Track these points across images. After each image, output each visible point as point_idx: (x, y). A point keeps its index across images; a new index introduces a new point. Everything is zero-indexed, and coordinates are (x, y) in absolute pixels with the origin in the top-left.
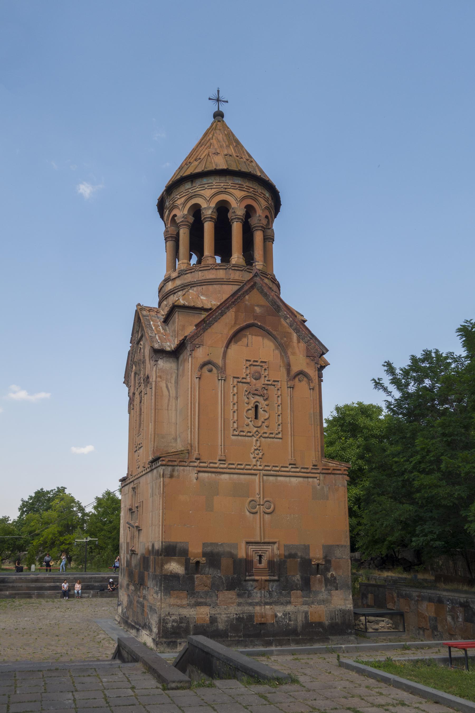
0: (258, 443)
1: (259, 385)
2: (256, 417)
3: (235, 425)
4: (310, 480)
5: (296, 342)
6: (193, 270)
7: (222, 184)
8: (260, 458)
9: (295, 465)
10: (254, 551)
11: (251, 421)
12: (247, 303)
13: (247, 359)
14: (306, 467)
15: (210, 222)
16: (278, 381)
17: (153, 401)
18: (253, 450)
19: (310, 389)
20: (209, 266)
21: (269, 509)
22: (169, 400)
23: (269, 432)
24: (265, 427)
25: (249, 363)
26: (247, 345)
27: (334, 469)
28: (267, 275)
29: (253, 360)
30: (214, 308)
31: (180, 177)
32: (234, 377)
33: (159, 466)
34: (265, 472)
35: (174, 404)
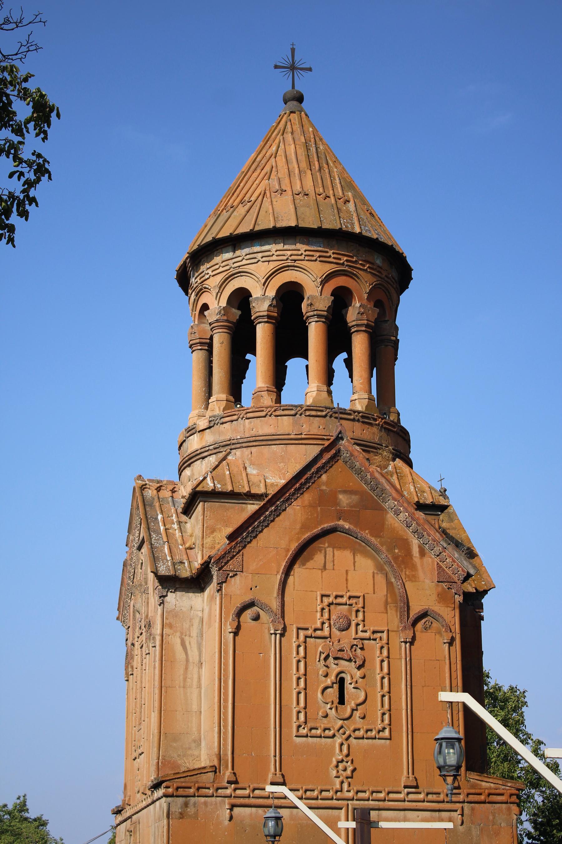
0: (345, 748)
1: (346, 641)
2: (342, 701)
3: (302, 716)
5: (418, 555)
6: (235, 417)
7: (289, 253)
8: (347, 778)
9: (417, 787)
12: (324, 488)
13: (324, 593)
14: (435, 790)
15: (267, 324)
16: (383, 632)
17: (157, 671)
18: (334, 762)
19: (445, 643)
20: (263, 411)
22: (186, 669)
24: (357, 718)
25: (326, 601)
26: (325, 567)
27: (489, 794)
28: (375, 420)
29: (334, 594)
30: (272, 492)
31: (209, 239)
33: (162, 797)
34: (358, 802)
35: (196, 676)
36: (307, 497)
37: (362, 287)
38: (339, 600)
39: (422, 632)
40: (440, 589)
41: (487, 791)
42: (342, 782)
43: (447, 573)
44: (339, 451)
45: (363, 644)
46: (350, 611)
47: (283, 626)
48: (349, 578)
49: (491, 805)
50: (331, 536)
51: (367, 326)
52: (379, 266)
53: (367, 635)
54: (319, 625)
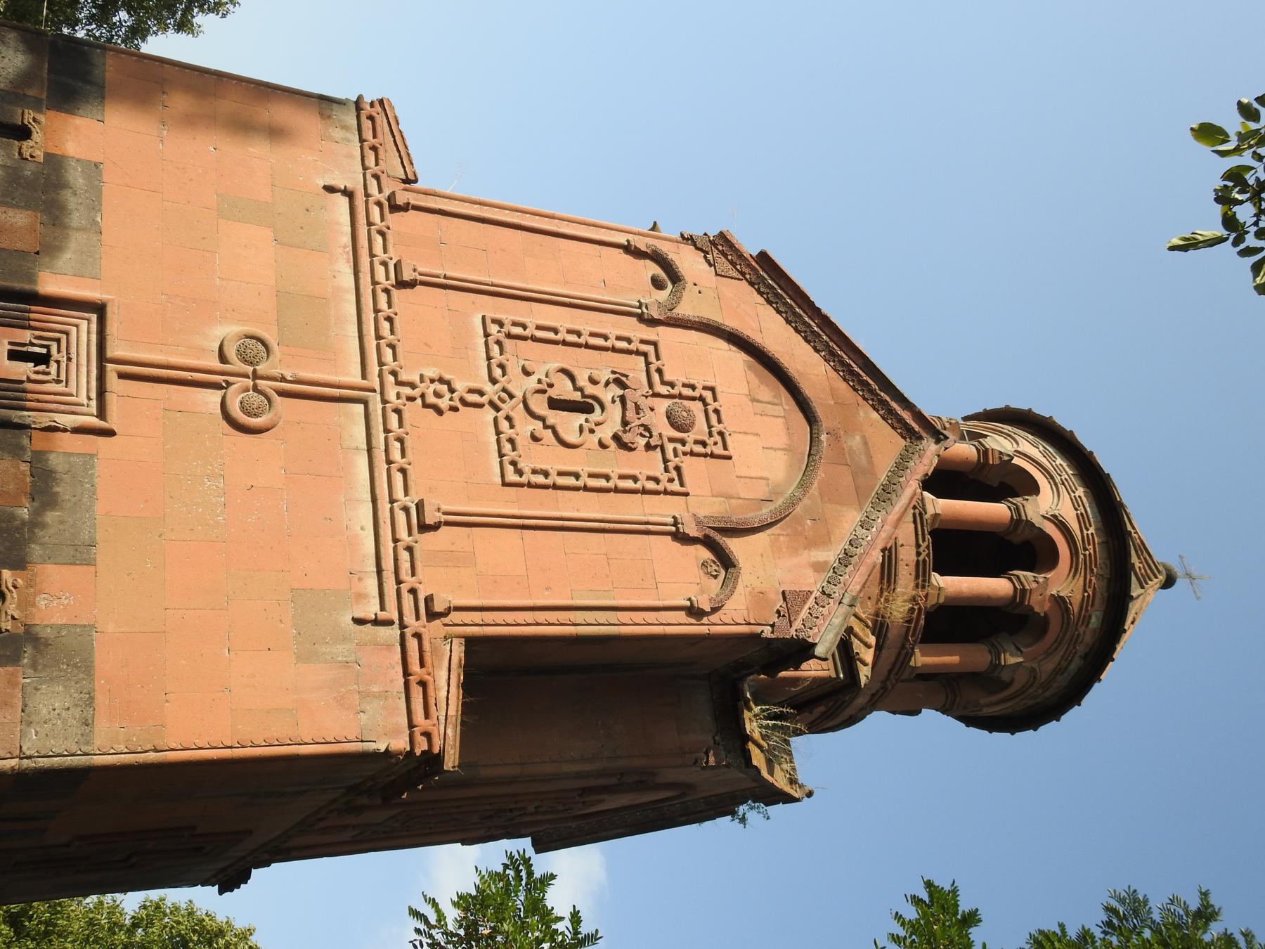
3: (517, 330)
4: (372, 583)
5: (813, 559)
8: (423, 396)
10: (67, 333)
11: (539, 381)
12: (862, 414)
13: (718, 390)
14: (419, 564)
16: (682, 484)
18: (447, 377)
19: (689, 599)
21: (242, 409)
23: (519, 441)
24: (531, 428)
25: (708, 395)
26: (754, 400)
27: (423, 684)
32: (655, 344)
34: (380, 412)
36: (843, 387)
37: (1061, 583)
38: (713, 418)
40: (772, 596)
42: (413, 386)
43: (802, 608)
44: (920, 438)
45: (656, 447)
46: (701, 433)
48: (750, 438)
50: (800, 416)
51: (1024, 590)
52: (1090, 617)
53: (670, 455)
54: (667, 378)
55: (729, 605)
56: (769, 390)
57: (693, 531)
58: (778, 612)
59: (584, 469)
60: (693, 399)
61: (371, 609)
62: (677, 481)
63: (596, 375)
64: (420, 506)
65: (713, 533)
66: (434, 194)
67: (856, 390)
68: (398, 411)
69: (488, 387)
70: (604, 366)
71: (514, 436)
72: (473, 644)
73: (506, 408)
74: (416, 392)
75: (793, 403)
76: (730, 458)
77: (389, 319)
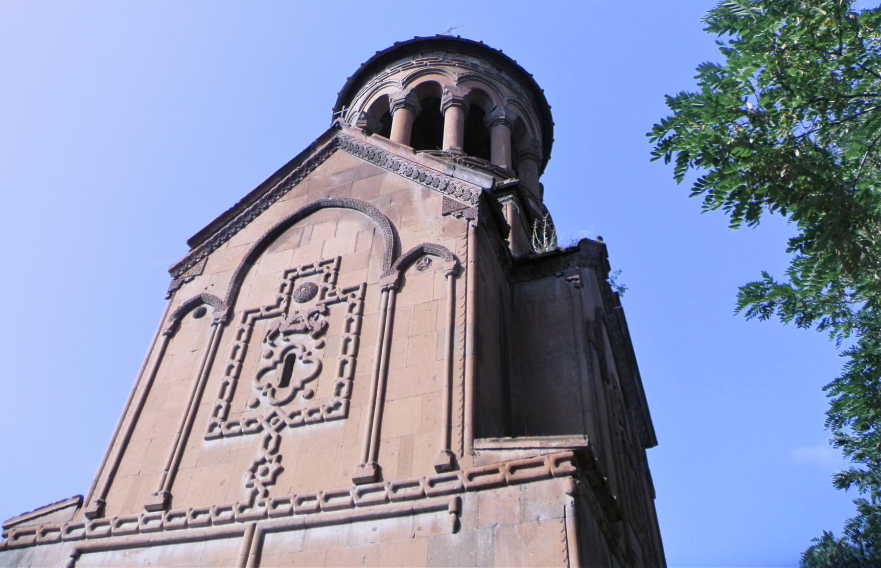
3: (221, 413)
4: (424, 519)
11: (265, 394)
13: (288, 268)
18: (251, 465)
19: (447, 276)
25: (290, 276)
26: (299, 245)
27: (513, 469)
32: (247, 313)
34: (274, 520)
38: (308, 271)
39: (415, 274)
41: (507, 466)
42: (255, 493)
44: (337, 140)
46: (319, 278)
47: (225, 312)
49: (518, 487)
50: (315, 216)
55: (453, 250)
56: (292, 235)
57: (394, 277)
58: (458, 217)
59: (340, 357)
60: (292, 285)
61: (446, 518)
62: (355, 293)
63: (265, 352)
64: (358, 481)
65: (396, 264)
66: (97, 481)
67: (299, 182)
68: (275, 504)
69: (264, 434)
70: (259, 348)
71: (307, 411)
72: (478, 433)
73: (283, 417)
74: (261, 490)
75: (303, 221)
76: (340, 258)
77: (195, 514)
